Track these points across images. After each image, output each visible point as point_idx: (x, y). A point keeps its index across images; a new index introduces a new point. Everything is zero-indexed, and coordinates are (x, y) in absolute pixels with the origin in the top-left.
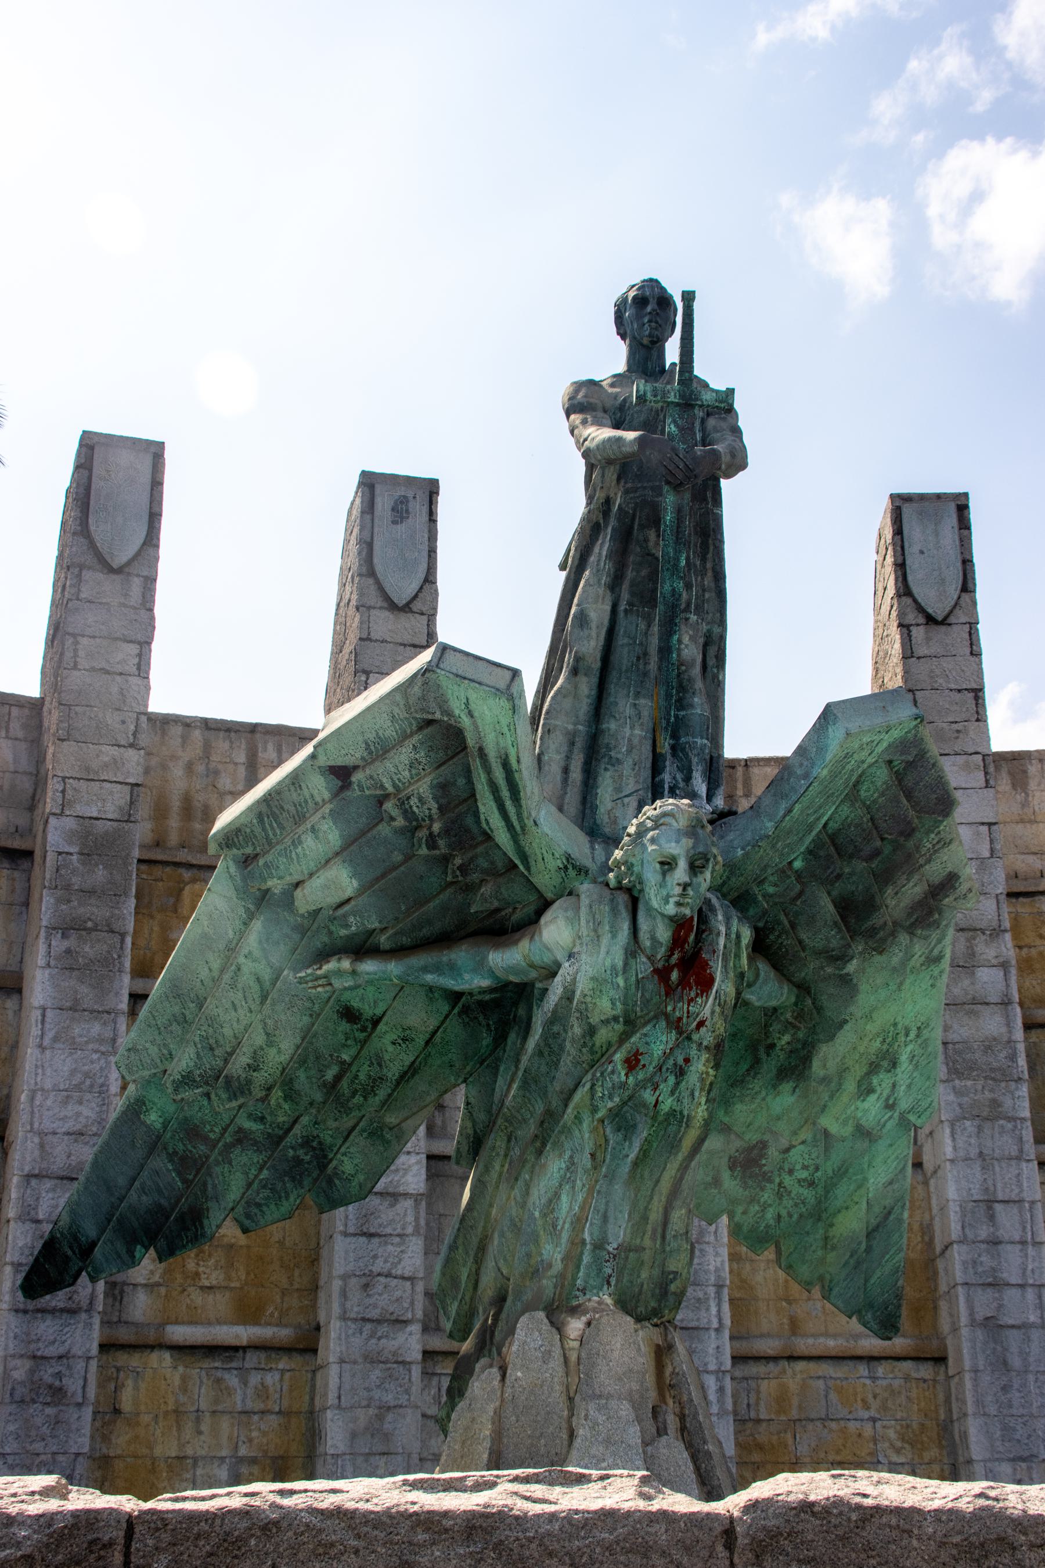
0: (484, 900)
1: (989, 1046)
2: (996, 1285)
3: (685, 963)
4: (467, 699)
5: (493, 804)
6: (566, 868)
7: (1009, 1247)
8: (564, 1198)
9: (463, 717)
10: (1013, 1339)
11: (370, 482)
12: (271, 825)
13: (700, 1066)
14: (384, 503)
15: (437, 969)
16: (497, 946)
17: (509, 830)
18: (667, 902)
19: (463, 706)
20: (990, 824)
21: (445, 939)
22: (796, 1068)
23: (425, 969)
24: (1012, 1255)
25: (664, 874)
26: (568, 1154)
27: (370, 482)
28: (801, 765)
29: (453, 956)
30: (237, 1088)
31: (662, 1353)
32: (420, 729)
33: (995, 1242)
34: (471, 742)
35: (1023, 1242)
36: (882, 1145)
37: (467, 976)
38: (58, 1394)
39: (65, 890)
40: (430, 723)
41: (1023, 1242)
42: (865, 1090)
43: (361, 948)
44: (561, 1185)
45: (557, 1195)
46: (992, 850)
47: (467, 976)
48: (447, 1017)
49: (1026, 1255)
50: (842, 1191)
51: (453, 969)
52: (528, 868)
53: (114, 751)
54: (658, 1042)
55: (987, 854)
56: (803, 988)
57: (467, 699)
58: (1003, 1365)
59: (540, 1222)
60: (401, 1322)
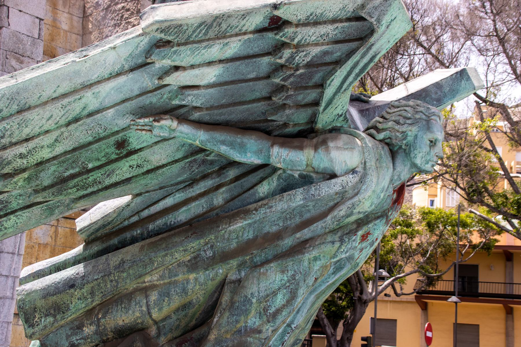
4: (395, 18)
5: (345, 73)
6: (341, 115)
7: (6, 255)
8: (280, 296)
9: (384, 26)
12: (201, 31)
15: (231, 145)
16: (283, 145)
17: (338, 88)
18: (427, 163)
19: (390, 20)
20: (41, 20)
21: (244, 127)
23: (223, 143)
25: (430, 147)
26: (290, 273)
28: (436, 93)
29: (245, 140)
32: (349, 20)
34: (372, 40)
35: (13, 254)
37: (249, 155)
40: (360, 19)
41: (13, 254)
44: (279, 289)
45: (275, 293)
46: (39, 34)
47: (249, 155)
48: (176, 161)
49: (13, 261)
51: (242, 148)
52: (324, 110)
55: (36, 36)
57: (395, 18)
59: (255, 305)
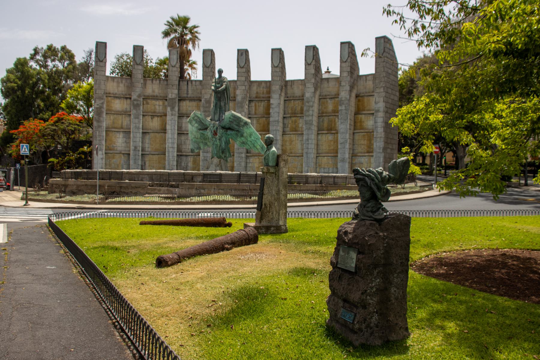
0: (206, 127)
1: (310, 121)
2: (308, 148)
3: (215, 134)
10: (309, 155)
11: (238, 50)
13: (218, 141)
14: (240, 54)
22: (242, 136)
24: (310, 145)
27: (238, 50)
30: (198, 139)
31: (220, 161)
33: (308, 144)
36: (257, 141)
38: (207, 160)
39: (204, 107)
42: (250, 137)
43: (200, 130)
50: (256, 145)
53: (208, 90)
54: (214, 139)
56: (237, 131)
58: (307, 157)
60: (242, 153)
